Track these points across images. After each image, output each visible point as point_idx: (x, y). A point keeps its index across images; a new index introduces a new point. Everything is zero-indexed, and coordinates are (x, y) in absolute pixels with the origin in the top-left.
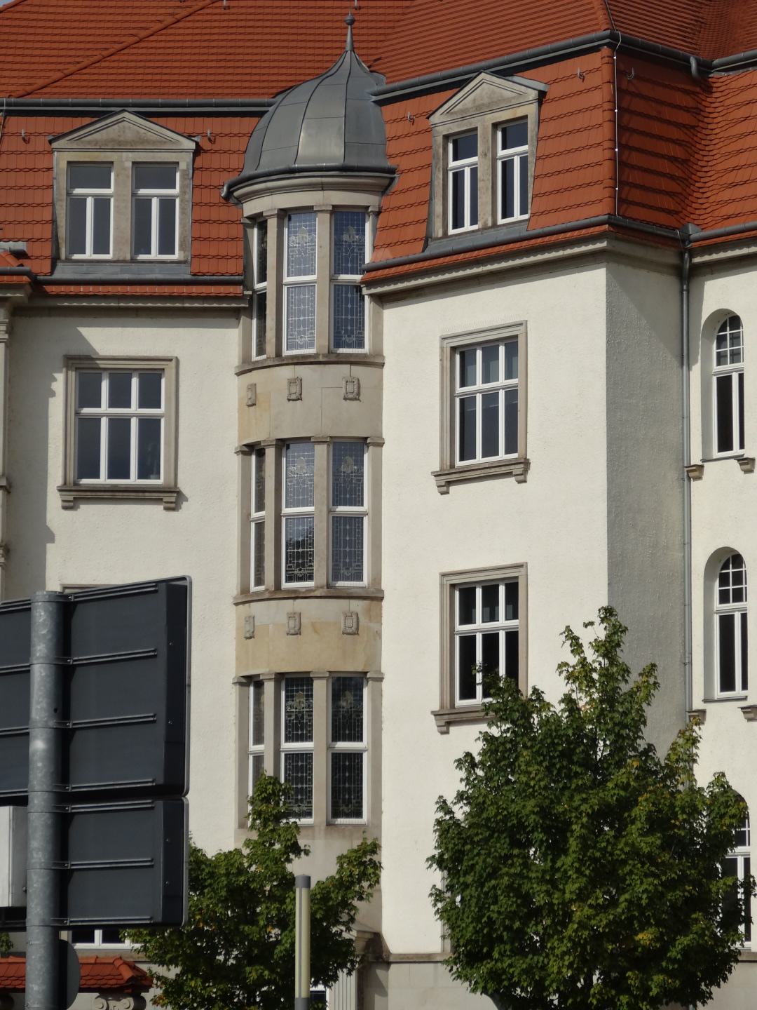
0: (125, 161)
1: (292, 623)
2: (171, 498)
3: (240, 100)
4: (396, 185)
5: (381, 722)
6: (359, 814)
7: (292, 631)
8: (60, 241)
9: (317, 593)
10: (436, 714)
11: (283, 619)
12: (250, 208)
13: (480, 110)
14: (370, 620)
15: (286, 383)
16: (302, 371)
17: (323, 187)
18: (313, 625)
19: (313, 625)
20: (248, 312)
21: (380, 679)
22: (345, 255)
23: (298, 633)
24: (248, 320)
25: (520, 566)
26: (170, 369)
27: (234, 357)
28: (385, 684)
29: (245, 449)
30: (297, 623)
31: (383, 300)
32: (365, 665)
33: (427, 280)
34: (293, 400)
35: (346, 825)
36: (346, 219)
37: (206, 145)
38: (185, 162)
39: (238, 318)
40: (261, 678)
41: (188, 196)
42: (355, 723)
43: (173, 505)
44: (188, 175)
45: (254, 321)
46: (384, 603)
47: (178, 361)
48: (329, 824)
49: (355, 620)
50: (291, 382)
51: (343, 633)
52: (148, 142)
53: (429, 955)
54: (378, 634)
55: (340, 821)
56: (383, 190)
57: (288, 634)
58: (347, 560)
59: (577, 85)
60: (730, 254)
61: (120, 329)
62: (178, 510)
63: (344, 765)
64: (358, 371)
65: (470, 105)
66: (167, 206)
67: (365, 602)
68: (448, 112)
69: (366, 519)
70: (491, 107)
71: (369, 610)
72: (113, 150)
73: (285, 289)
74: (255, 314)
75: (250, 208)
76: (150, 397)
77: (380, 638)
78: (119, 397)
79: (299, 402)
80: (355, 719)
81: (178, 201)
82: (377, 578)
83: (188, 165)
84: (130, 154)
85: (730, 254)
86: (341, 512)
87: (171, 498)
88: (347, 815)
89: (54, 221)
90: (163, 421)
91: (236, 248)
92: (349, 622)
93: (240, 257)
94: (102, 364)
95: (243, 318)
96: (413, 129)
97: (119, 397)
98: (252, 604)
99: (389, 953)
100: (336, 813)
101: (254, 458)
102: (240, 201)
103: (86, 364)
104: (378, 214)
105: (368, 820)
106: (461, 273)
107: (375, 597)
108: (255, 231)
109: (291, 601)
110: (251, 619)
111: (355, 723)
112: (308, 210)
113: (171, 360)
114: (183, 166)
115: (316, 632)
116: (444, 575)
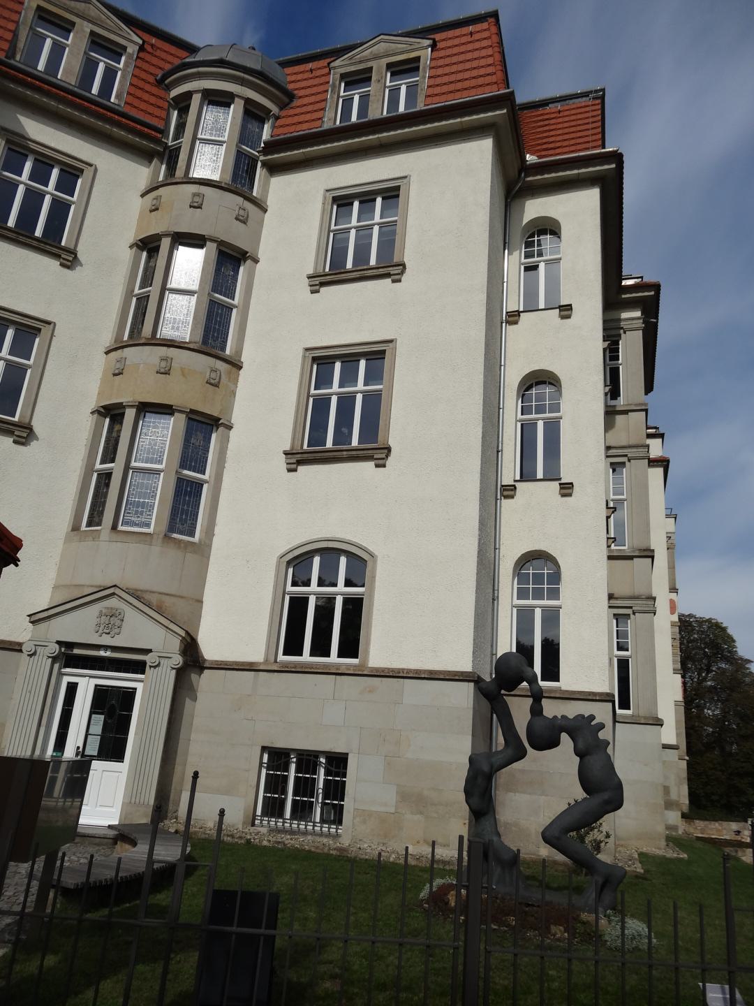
0: (87, 27)
1: (163, 364)
2: (69, 259)
4: (296, 103)
5: (225, 462)
6: (192, 534)
7: (162, 370)
8: (18, 50)
9: (191, 346)
10: (286, 453)
11: (156, 361)
12: (175, 93)
13: (377, 57)
14: (229, 381)
15: (190, 196)
16: (204, 189)
17: (243, 82)
18: (182, 370)
19: (182, 370)
20: (160, 156)
21: (230, 428)
22: (245, 137)
23: (167, 373)
24: (159, 163)
25: (391, 341)
26: (88, 173)
27: (143, 184)
28: (232, 433)
29: (140, 243)
30: (169, 364)
31: (275, 169)
32: (220, 413)
34: (195, 207)
35: (180, 541)
36: (253, 114)
37: (148, 47)
38: (132, 49)
39: (150, 162)
40: (124, 404)
41: (131, 69)
42: (200, 459)
43: (69, 264)
44: (132, 58)
45: (164, 167)
46: (241, 372)
47: (96, 170)
48: (166, 537)
49: (219, 374)
50: (195, 195)
51: (207, 382)
52: (106, 23)
53: (251, 664)
54: (234, 393)
55: (175, 535)
56: (283, 106)
57: (157, 372)
58: (215, 335)
61: (53, 130)
62: (72, 270)
63: (186, 490)
64: (248, 205)
66: (110, 74)
67: (227, 365)
69: (235, 311)
71: (229, 373)
73: (198, 142)
74: (165, 162)
75: (175, 93)
76: (67, 184)
77: (235, 397)
78: (40, 175)
79: (199, 210)
80: (201, 456)
81: (119, 73)
82: (239, 352)
83: (134, 51)
84: (90, 25)
86: (215, 298)
87: (69, 259)
88: (181, 533)
89: (15, 34)
90: (73, 207)
91: (163, 114)
92: (213, 375)
93: (163, 119)
94: (32, 146)
95: (155, 161)
96: (311, 76)
97: (40, 175)
98: (125, 349)
99: (205, 660)
100: (172, 528)
101: (145, 254)
102: (169, 88)
103: (16, 139)
105: (200, 540)
107: (235, 365)
108: (176, 112)
109: (165, 348)
110: (122, 360)
111: (200, 459)
113: (91, 165)
115: (183, 375)
116: (307, 349)
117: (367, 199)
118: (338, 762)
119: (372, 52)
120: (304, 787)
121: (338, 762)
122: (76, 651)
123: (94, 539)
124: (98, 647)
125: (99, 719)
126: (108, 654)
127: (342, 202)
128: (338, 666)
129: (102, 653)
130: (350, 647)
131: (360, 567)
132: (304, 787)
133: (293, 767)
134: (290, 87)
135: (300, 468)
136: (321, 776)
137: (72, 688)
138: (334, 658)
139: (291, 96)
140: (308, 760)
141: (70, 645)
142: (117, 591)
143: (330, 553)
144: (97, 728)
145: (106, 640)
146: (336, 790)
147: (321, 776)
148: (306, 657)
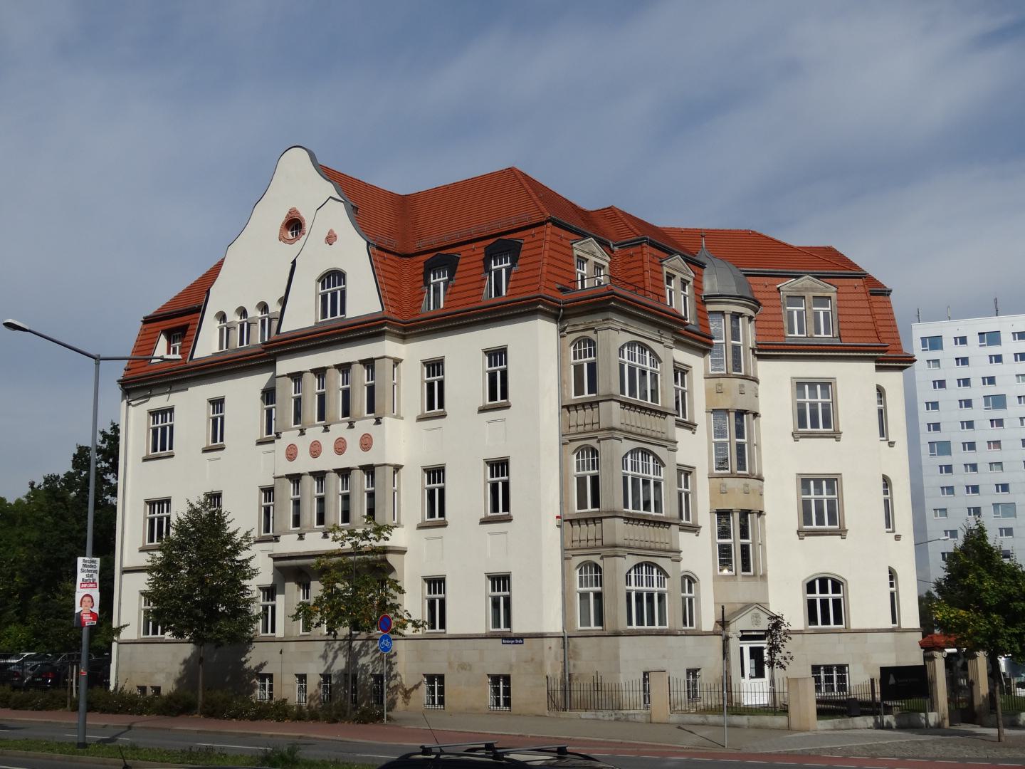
3: (791, 271)
13: (807, 289)
33: (784, 353)
38: (691, 283)
59: (851, 289)
60: (887, 364)
65: (800, 286)
68: (789, 287)
70: (813, 290)
72: (677, 271)
85: (887, 364)
96: (766, 290)
104: (756, 321)
106: (807, 354)
110: (725, 485)
112: (723, 313)
114: (691, 283)
116: (799, 474)
117: (812, 385)
118: (842, 668)
119: (803, 285)
120: (829, 679)
121: (842, 668)
122: (744, 634)
123: (734, 580)
124: (751, 631)
125: (753, 660)
126: (755, 633)
127: (800, 385)
128: (834, 629)
129: (753, 633)
130: (838, 620)
131: (837, 586)
132: (829, 679)
133: (822, 673)
134: (760, 301)
135: (806, 538)
136: (835, 674)
137: (742, 649)
138: (832, 625)
139: (759, 305)
140: (828, 669)
141: (742, 631)
142: (758, 606)
143: (823, 581)
144: (753, 665)
145: (756, 628)
146: (842, 679)
147: (835, 674)
148: (832, 625)
